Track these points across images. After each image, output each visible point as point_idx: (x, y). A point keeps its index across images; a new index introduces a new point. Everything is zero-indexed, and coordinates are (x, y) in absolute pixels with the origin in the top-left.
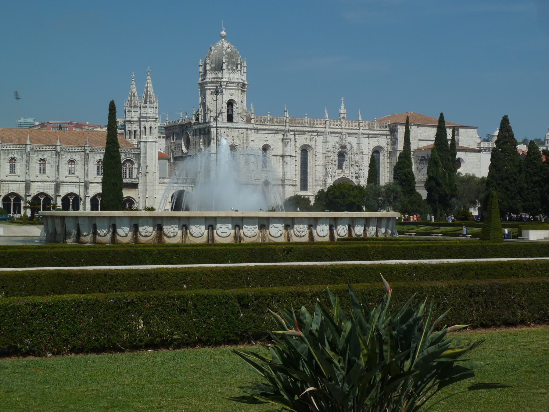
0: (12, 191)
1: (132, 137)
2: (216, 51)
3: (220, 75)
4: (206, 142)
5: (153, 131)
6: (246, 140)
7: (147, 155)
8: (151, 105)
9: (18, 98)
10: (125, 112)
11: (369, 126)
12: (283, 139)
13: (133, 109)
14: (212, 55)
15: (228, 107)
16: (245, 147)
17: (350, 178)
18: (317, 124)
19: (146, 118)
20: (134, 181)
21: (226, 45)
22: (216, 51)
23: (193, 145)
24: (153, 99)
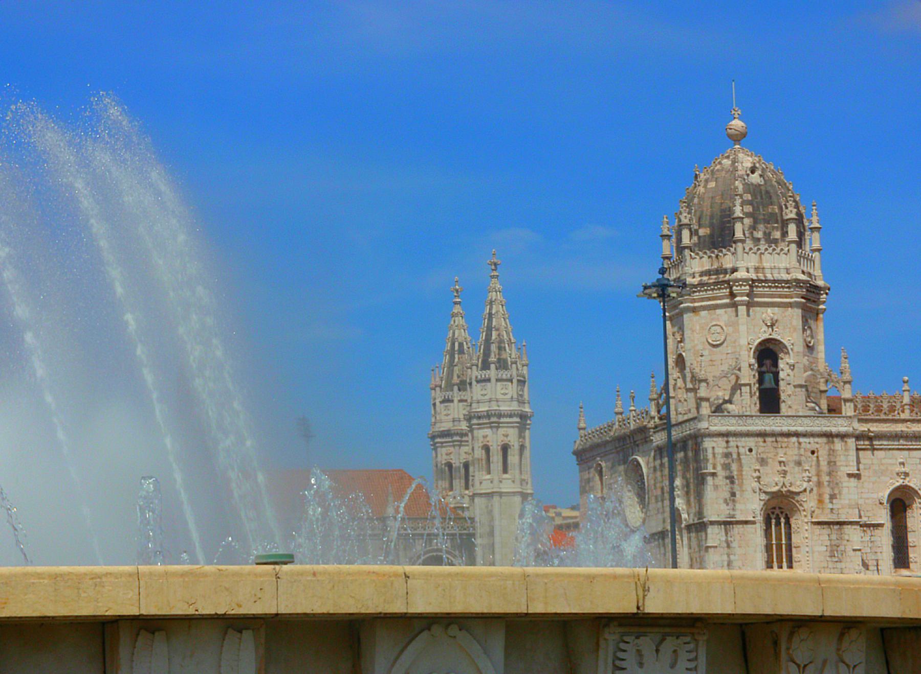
1: (458, 483)
2: (712, 185)
3: (728, 261)
4: (692, 487)
5: (513, 459)
6: (829, 474)
7: (497, 539)
8: (505, 374)
10: (434, 405)
13: (456, 395)
14: (701, 198)
15: (760, 362)
16: (826, 497)
19: (488, 415)
21: (746, 161)
22: (712, 185)
23: (657, 502)
24: (511, 353)
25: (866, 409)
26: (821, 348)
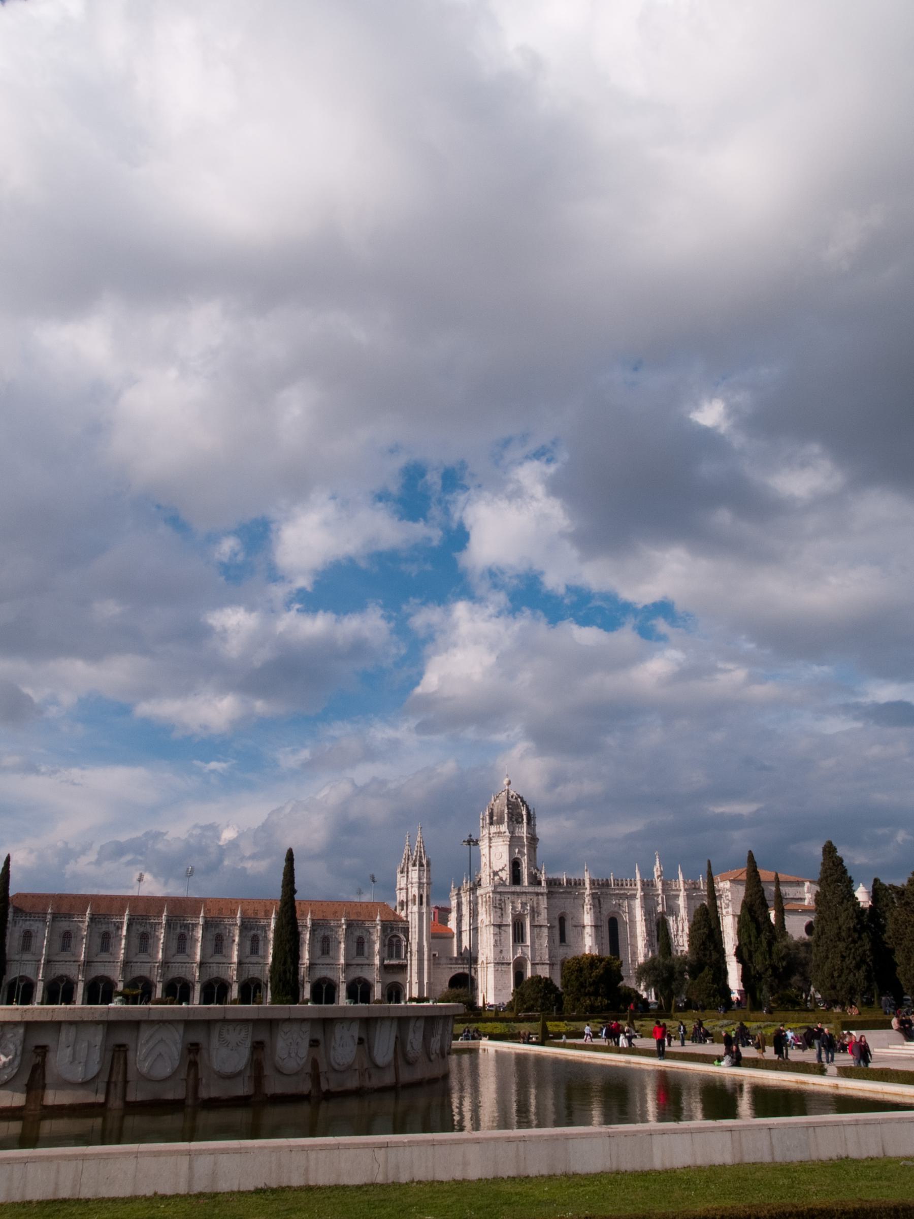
0: (252, 976)
2: (498, 801)
5: (425, 900)
9: (373, 881)
18: (627, 885)
20: (401, 962)
25: (551, 883)
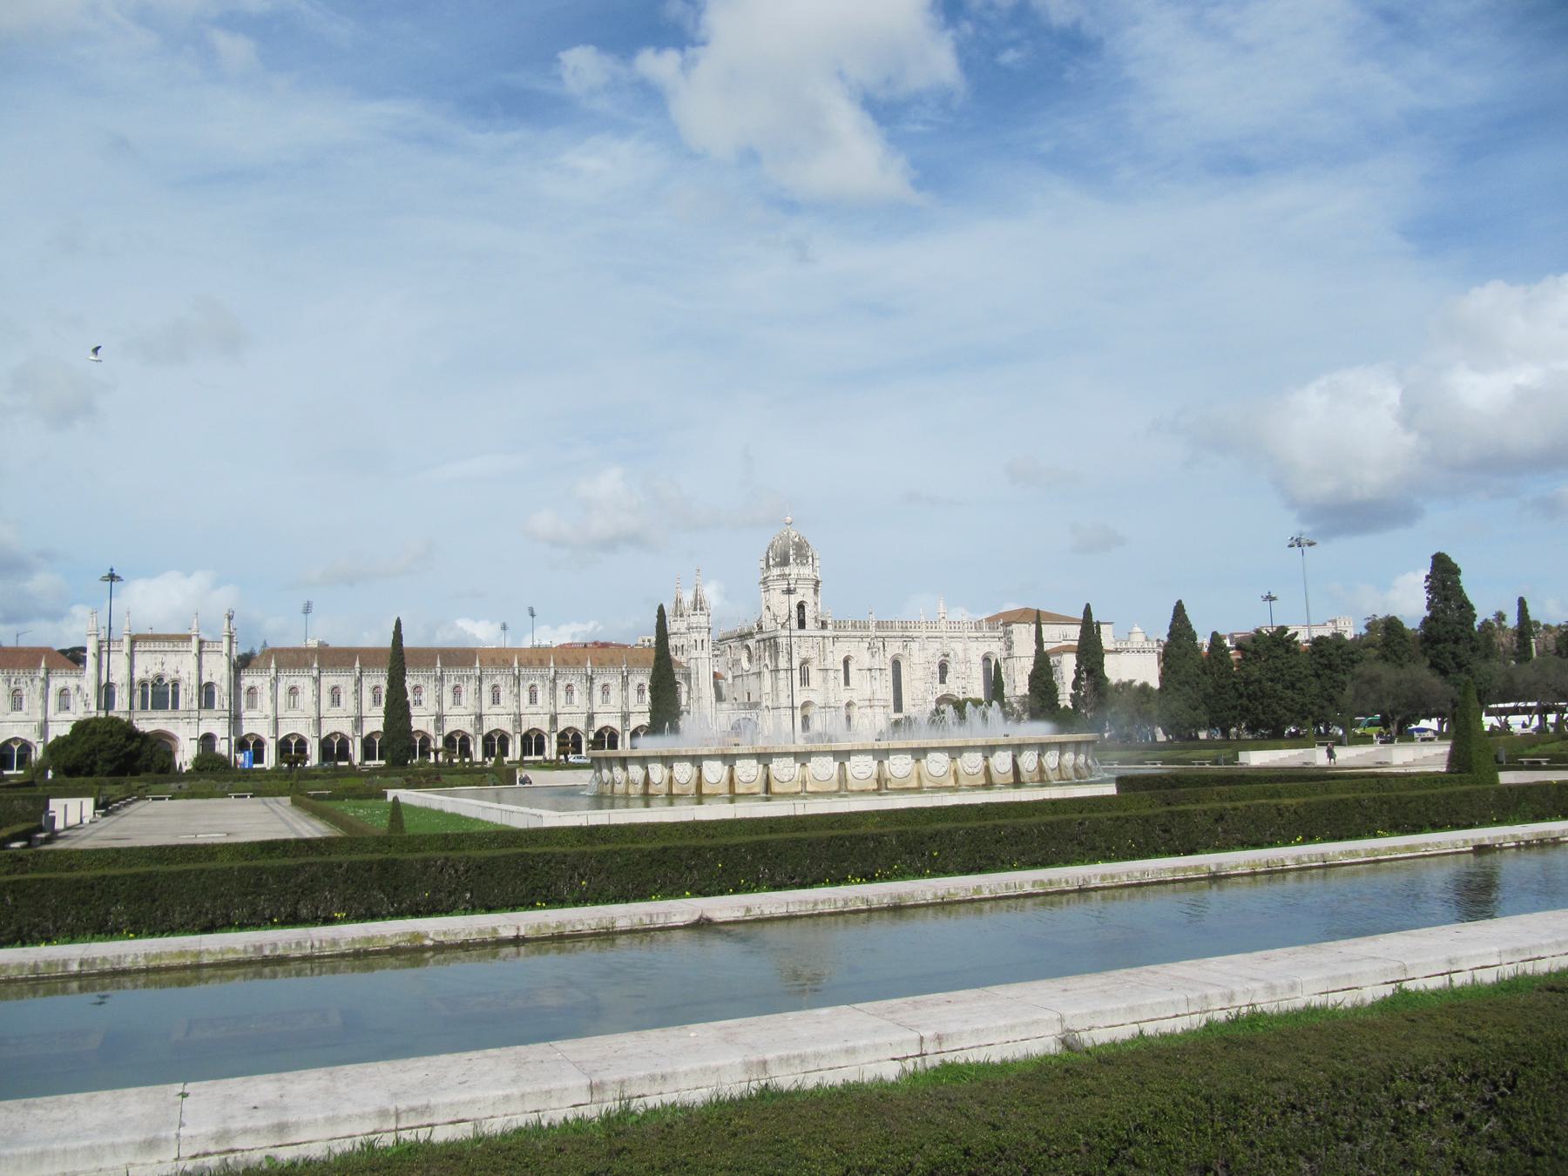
2: (780, 542)
3: (787, 573)
5: (705, 645)
8: (702, 612)
11: (976, 628)
12: (868, 648)
17: (956, 694)
25: (836, 627)
26: (819, 604)
